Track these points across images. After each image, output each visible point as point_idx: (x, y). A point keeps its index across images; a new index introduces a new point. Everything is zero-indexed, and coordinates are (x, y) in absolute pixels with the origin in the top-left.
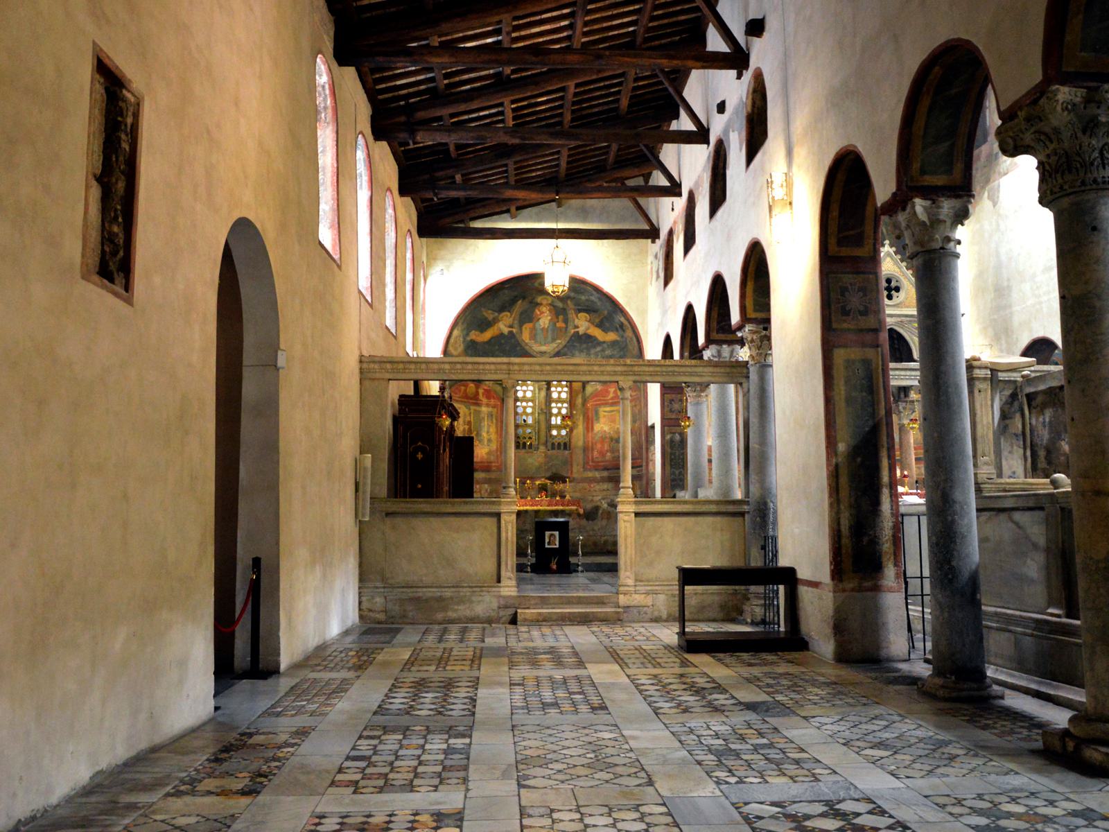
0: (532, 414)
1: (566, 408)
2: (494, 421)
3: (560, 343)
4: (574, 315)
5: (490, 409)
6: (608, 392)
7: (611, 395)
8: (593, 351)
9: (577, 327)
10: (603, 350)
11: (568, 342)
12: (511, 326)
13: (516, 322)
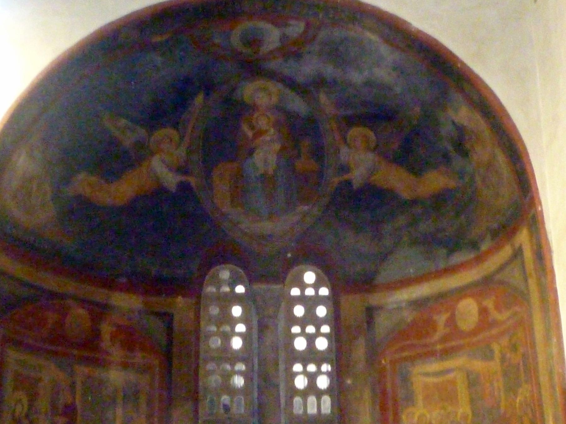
0: (246, 390)
1: (328, 374)
2: (143, 407)
5: (132, 376)
7: (441, 330)
9: (344, 169)
12: (183, 169)
13: (196, 157)
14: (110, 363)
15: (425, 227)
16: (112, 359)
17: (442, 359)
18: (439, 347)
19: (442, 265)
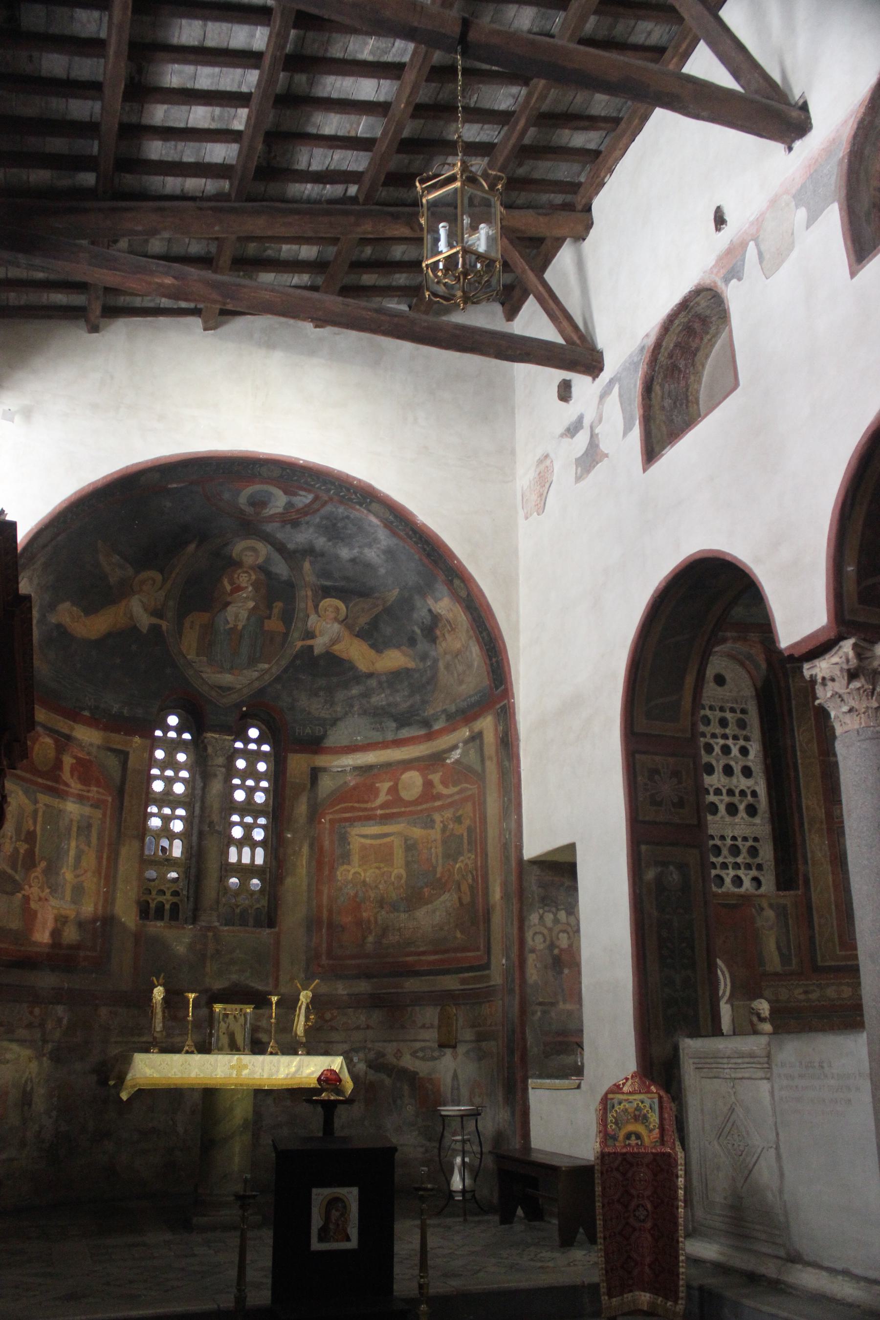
2: (94, 840)
3: (267, 671)
5: (87, 810)
7: (382, 798)
8: (340, 695)
11: (285, 670)
14: (67, 793)
15: (379, 699)
16: (71, 790)
17: (381, 824)
18: (379, 812)
19: (390, 736)
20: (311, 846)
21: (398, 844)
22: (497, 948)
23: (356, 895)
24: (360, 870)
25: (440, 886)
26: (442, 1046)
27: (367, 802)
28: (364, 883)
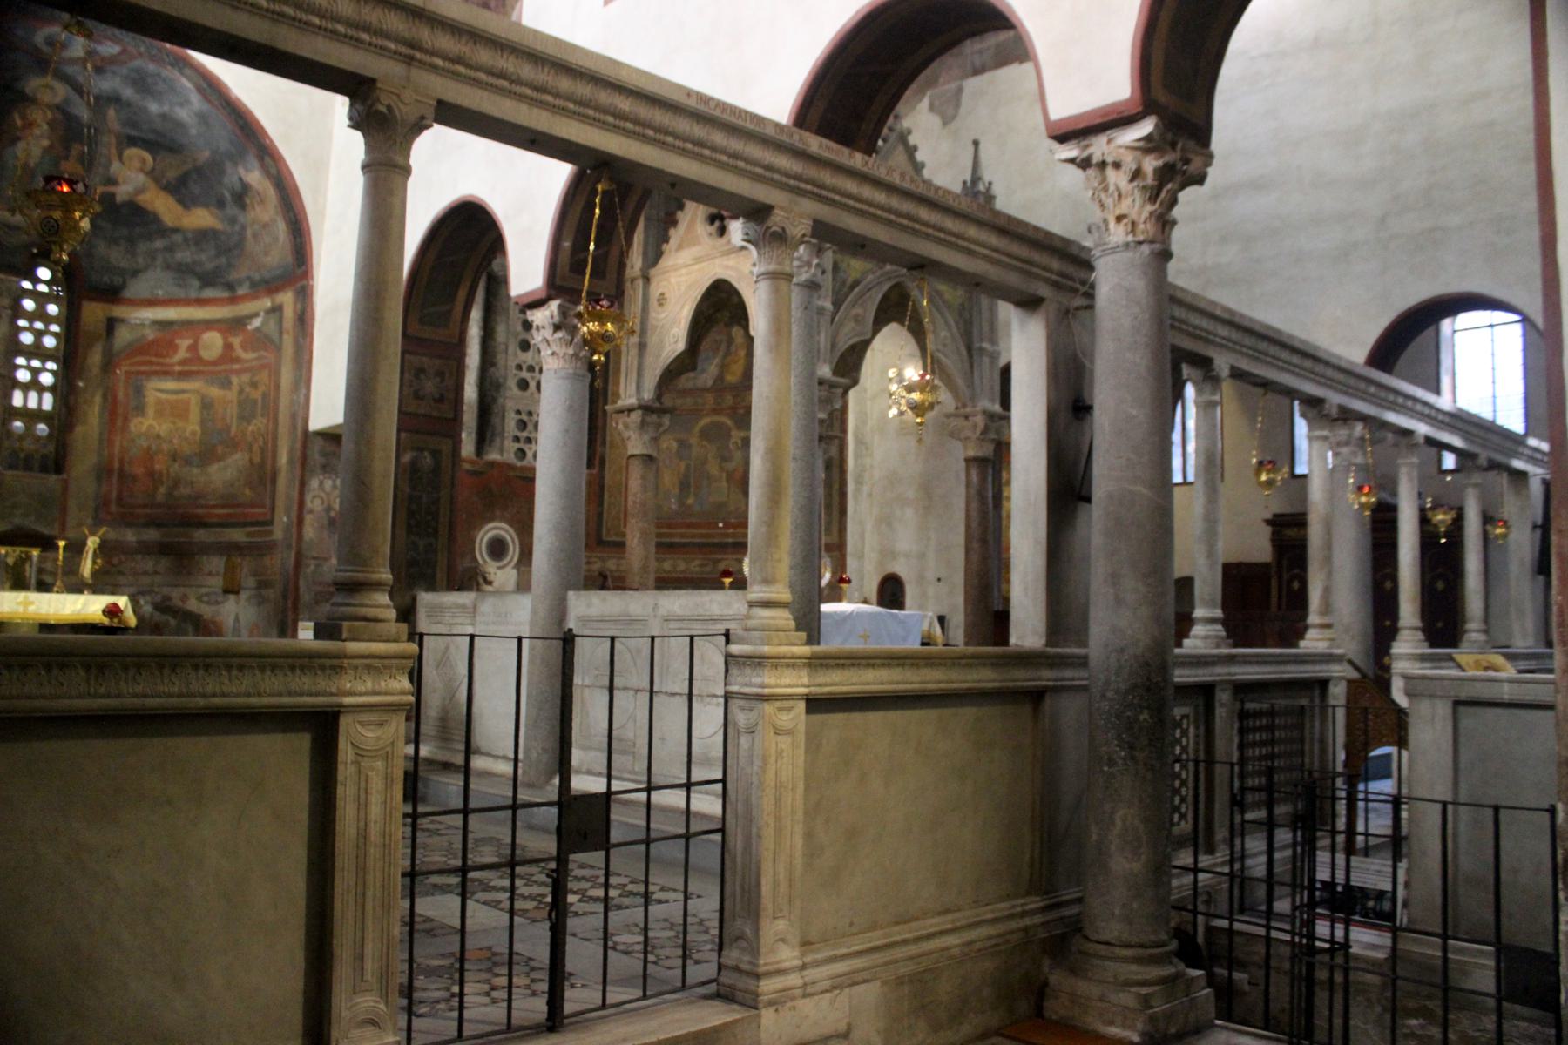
4: (113, 150)
6: (175, 348)
7: (182, 354)
10: (170, 249)
15: (183, 256)
18: (177, 368)
19: (193, 295)
20: (105, 397)
21: (194, 401)
22: (280, 503)
23: (149, 448)
24: (154, 423)
25: (233, 445)
26: (226, 591)
27: (162, 356)
28: (158, 436)
